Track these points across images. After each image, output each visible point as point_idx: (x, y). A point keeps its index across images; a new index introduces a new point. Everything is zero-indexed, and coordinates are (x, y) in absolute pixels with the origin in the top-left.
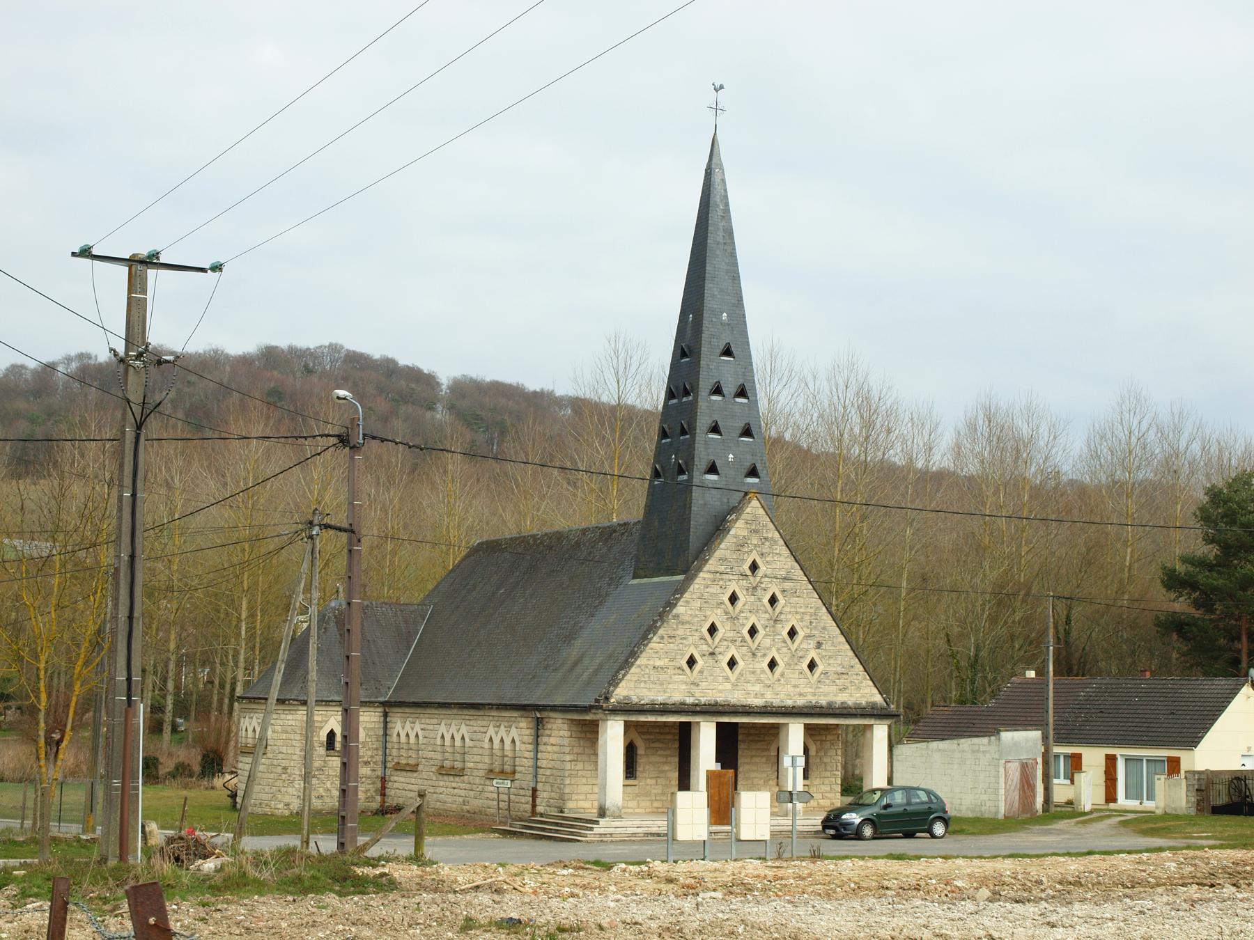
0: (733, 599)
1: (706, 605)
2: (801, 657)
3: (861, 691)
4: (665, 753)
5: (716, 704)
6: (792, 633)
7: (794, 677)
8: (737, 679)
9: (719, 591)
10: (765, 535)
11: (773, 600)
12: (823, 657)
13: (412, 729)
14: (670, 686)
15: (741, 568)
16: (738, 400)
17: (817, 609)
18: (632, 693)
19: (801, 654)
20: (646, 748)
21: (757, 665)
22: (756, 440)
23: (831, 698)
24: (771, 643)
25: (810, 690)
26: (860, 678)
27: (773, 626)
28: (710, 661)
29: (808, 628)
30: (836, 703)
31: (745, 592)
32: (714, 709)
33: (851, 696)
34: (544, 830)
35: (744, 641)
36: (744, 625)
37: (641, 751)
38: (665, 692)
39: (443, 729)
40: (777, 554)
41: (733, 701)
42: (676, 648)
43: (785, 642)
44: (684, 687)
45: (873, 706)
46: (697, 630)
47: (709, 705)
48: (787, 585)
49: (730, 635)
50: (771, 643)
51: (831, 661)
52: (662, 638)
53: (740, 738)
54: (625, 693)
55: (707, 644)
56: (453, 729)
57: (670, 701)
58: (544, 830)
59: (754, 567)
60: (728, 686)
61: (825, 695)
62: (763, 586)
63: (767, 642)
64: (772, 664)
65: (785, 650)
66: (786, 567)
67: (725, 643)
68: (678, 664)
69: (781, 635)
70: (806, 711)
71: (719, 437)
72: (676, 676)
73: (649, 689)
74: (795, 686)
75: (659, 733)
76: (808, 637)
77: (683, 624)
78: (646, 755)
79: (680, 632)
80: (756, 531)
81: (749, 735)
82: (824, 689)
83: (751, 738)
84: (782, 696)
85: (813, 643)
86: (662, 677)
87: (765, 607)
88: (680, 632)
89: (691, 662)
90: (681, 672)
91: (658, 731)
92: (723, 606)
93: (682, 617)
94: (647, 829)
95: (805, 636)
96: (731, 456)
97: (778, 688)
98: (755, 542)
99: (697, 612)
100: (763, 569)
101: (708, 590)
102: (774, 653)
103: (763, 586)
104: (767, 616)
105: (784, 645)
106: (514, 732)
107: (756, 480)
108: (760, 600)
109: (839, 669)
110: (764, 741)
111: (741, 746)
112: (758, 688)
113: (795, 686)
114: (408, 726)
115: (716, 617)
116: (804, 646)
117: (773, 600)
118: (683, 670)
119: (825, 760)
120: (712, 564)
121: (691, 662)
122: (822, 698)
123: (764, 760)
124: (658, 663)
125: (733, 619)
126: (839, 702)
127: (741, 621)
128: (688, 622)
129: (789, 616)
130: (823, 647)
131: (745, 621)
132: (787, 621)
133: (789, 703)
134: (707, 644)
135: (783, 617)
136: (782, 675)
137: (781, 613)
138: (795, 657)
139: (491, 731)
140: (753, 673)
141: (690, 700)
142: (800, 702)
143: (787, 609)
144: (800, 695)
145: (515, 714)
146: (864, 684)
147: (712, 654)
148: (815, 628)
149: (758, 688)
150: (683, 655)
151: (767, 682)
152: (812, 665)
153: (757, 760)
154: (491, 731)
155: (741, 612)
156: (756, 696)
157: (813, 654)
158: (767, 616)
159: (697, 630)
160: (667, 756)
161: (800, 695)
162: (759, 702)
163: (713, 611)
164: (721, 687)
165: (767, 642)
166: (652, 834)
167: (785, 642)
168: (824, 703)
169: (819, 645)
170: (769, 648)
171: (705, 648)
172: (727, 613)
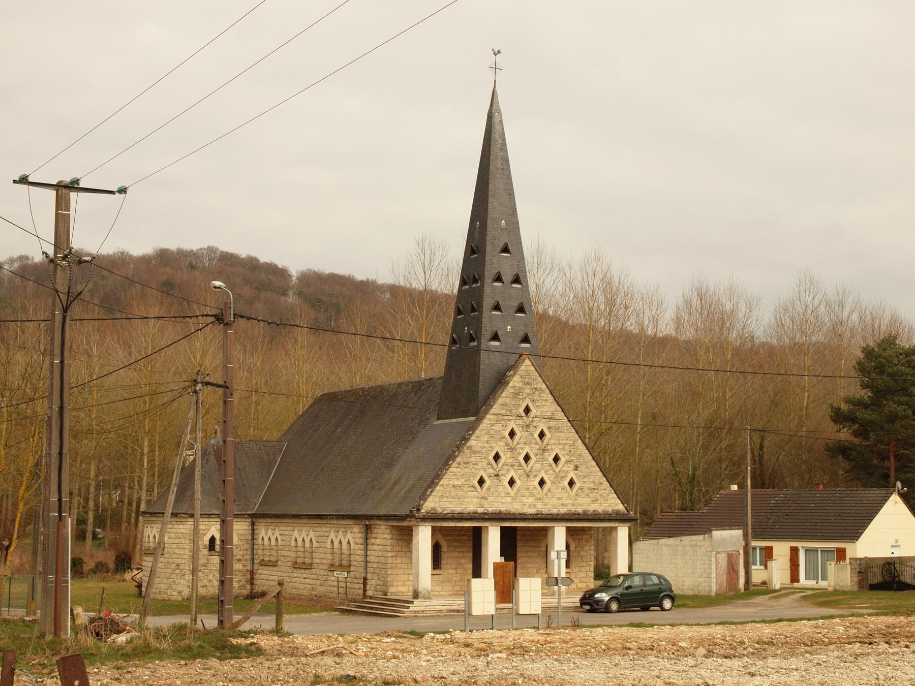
0: (512, 434)
1: (492, 439)
2: (563, 477)
4: (462, 550)
5: (500, 513)
6: (556, 459)
7: (558, 492)
9: (502, 428)
10: (535, 386)
11: (542, 435)
12: (579, 476)
13: (273, 534)
14: (466, 500)
15: (517, 411)
16: (514, 285)
17: (575, 441)
18: (437, 505)
19: (563, 474)
20: (448, 547)
21: (530, 484)
22: (528, 315)
23: (585, 507)
24: (541, 467)
25: (570, 501)
27: (542, 454)
28: (496, 481)
29: (568, 455)
31: (520, 429)
32: (499, 516)
33: (601, 505)
34: (372, 608)
35: (520, 465)
36: (520, 453)
37: (444, 549)
38: (462, 504)
39: (296, 534)
40: (544, 400)
41: (513, 511)
42: (470, 471)
43: (551, 466)
44: (476, 500)
45: (617, 513)
46: (485, 458)
47: (495, 513)
48: (552, 423)
49: (510, 461)
50: (541, 467)
51: (586, 480)
52: (459, 464)
53: (518, 538)
54: (432, 505)
55: (493, 468)
56: (304, 534)
57: (466, 511)
58: (372, 608)
59: (527, 410)
60: (509, 499)
61: (581, 505)
62: (534, 424)
63: (538, 466)
64: (542, 483)
65: (551, 472)
66: (551, 410)
67: (506, 467)
68: (472, 484)
70: (567, 517)
71: (500, 313)
72: (470, 493)
73: (450, 503)
74: (559, 499)
75: (457, 535)
76: (568, 462)
77: (475, 453)
78: (448, 551)
79: (473, 459)
80: (529, 383)
81: (524, 535)
82: (580, 500)
83: (526, 538)
84: (549, 507)
85: (571, 467)
86: (460, 493)
88: (473, 459)
89: (481, 482)
90: (473, 489)
91: (457, 533)
92: (504, 440)
93: (474, 448)
94: (449, 607)
95: (566, 461)
96: (509, 327)
99: (485, 445)
100: (534, 411)
101: (493, 428)
102: (542, 474)
103: (534, 424)
104: (537, 446)
105: (550, 468)
106: (349, 536)
107: (528, 345)
108: (532, 435)
109: (592, 486)
110: (536, 540)
111: (519, 544)
112: (531, 500)
113: (559, 499)
114: (270, 532)
115: (499, 447)
116: (566, 468)
117: (542, 435)
118: (475, 488)
119: (582, 553)
120: (496, 409)
121: (481, 482)
122: (579, 507)
123: (536, 554)
124: (456, 483)
125: (512, 449)
126: (591, 510)
127: (518, 451)
128: (479, 452)
129: (554, 447)
130: (580, 469)
131: (521, 451)
132: (552, 450)
133: (555, 511)
134: (493, 468)
135: (549, 447)
136: (549, 490)
137: (548, 444)
138: (559, 477)
139: (332, 535)
140: (528, 489)
141: (480, 510)
142: (563, 510)
143: (552, 441)
144: (563, 505)
145: (350, 522)
146: (610, 497)
147: (497, 475)
148: (574, 455)
149: (531, 500)
150: (474, 477)
151: (538, 496)
152: (571, 483)
153: (532, 554)
154: (332, 535)
155: (518, 444)
156: (530, 507)
157: (572, 475)
158: (537, 446)
159: (485, 458)
160: (463, 552)
161: (563, 505)
162: (532, 511)
163: (497, 443)
164: (503, 500)
165: (538, 466)
166: (453, 611)
167: (551, 466)
168: (580, 511)
169: (576, 468)
170: (539, 471)
171: (491, 471)
172: (507, 445)
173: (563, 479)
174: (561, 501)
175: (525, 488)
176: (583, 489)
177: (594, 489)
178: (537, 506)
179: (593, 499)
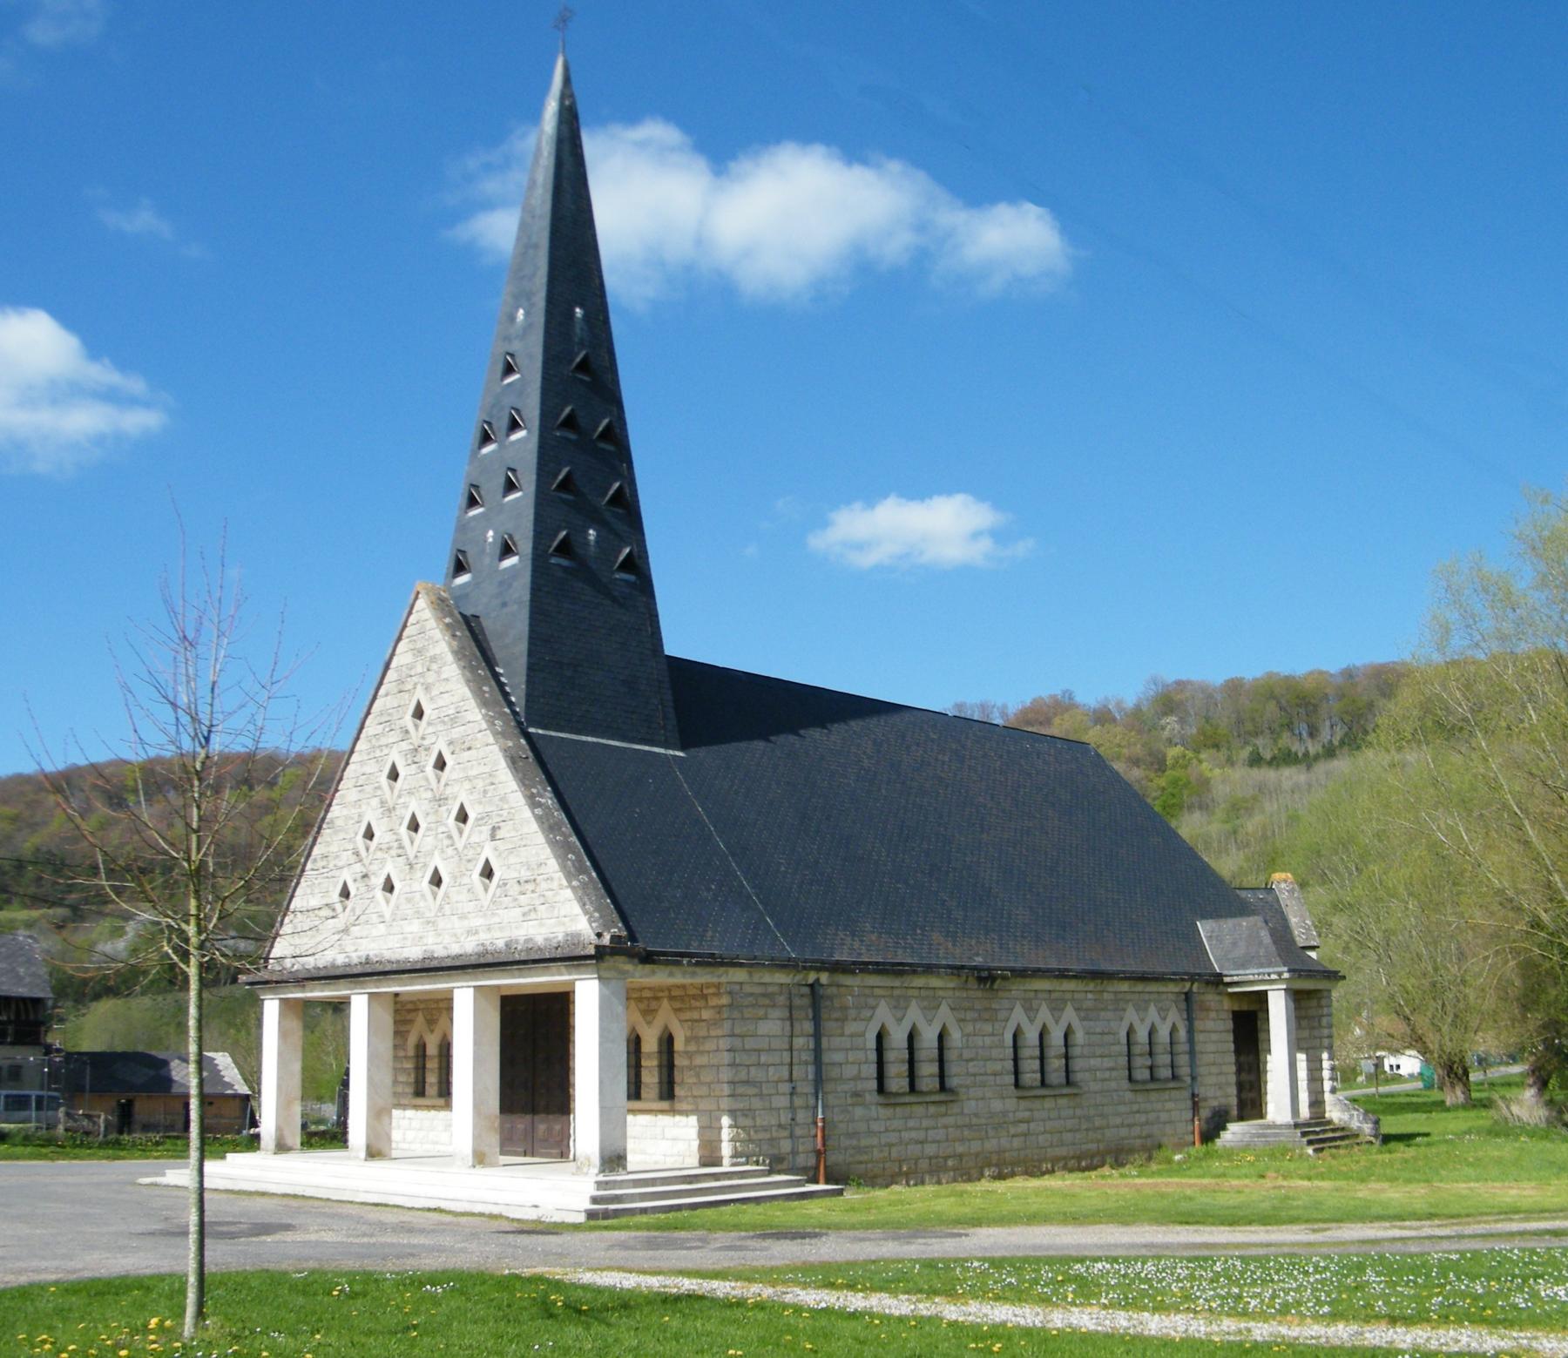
0: (394, 775)
2: (469, 861)
3: (556, 913)
6: (463, 817)
8: (393, 914)
11: (441, 764)
19: (470, 853)
24: (432, 849)
26: (555, 885)
29: (480, 803)
30: (517, 942)
33: (541, 925)
45: (574, 939)
48: (456, 733)
49: (389, 837)
51: (512, 860)
52: (315, 860)
59: (419, 713)
61: (501, 929)
62: (426, 743)
63: (430, 840)
64: (437, 880)
65: (450, 851)
66: (455, 699)
69: (446, 825)
74: (463, 917)
84: (447, 939)
85: (486, 830)
87: (427, 779)
89: (345, 893)
92: (379, 793)
95: (477, 820)
97: (442, 924)
98: (419, 669)
102: (437, 861)
103: (426, 743)
104: (429, 795)
105: (449, 842)
112: (414, 927)
115: (372, 815)
117: (441, 764)
126: (522, 939)
130: (500, 834)
131: (403, 811)
135: (449, 791)
137: (446, 785)
143: (455, 776)
144: (470, 932)
147: (365, 876)
152: (488, 873)
155: (399, 796)
157: (488, 852)
158: (429, 795)
161: (470, 932)
162: (413, 953)
164: (375, 932)
165: (430, 840)
170: (431, 854)
172: (383, 803)
173: (470, 866)
174: (466, 923)
175: (407, 899)
176: (505, 884)
177: (526, 882)
178: (425, 941)
179: (526, 909)
